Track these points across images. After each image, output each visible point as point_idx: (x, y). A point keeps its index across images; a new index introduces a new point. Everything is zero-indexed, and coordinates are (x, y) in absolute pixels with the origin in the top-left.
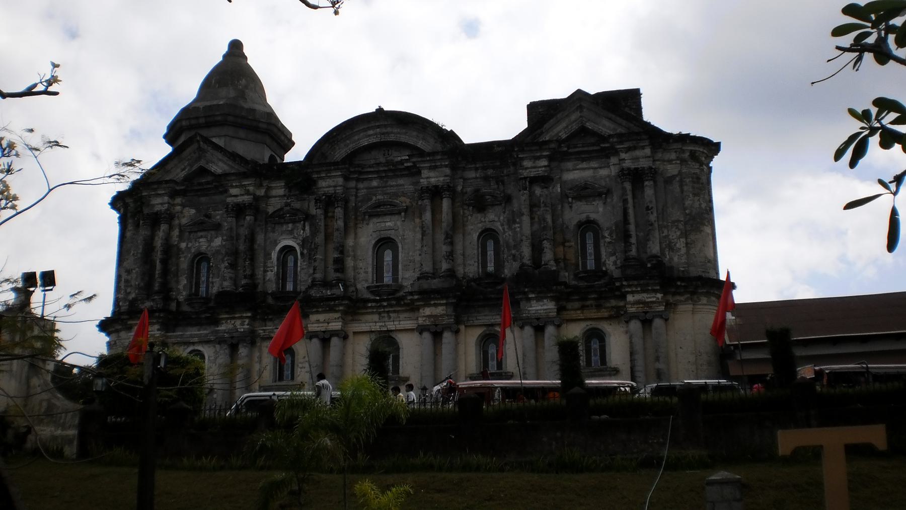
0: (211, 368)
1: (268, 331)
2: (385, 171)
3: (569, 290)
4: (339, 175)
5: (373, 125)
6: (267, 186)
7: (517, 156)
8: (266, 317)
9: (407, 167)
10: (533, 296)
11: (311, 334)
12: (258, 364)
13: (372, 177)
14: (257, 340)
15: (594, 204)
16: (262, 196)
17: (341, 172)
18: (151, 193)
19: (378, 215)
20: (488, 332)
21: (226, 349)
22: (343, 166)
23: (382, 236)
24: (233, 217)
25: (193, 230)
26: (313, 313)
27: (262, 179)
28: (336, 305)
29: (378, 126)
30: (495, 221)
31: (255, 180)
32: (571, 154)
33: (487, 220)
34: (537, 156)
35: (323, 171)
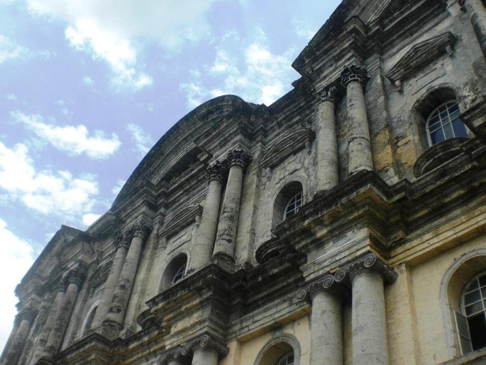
2: (187, 180)
3: (397, 197)
4: (143, 203)
5: (181, 140)
6: (97, 250)
7: (313, 71)
10: (324, 231)
13: (179, 196)
15: (436, 68)
20: (273, 343)
22: (143, 190)
23: (175, 255)
24: (61, 291)
27: (92, 243)
29: (185, 139)
30: (296, 170)
31: (83, 246)
32: (391, 32)
33: (287, 173)
34: (337, 55)
35: (128, 206)
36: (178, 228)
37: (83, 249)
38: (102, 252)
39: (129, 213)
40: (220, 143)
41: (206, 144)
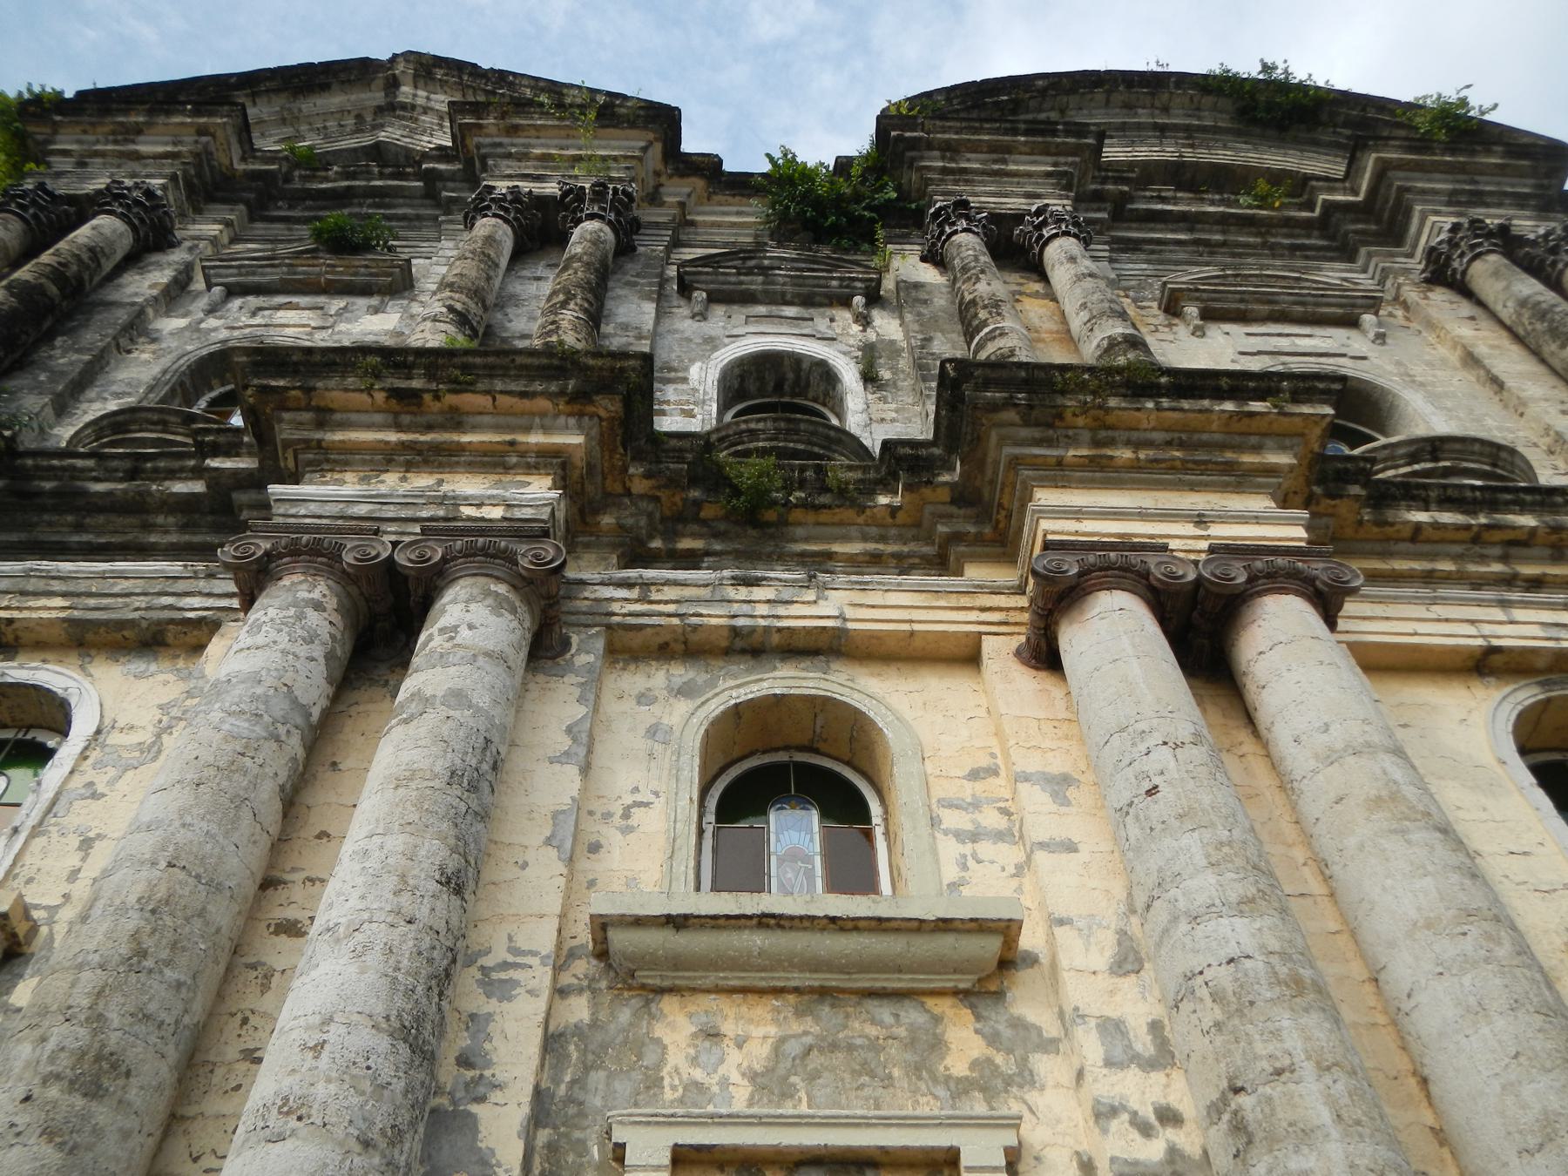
0: (95, 796)
1: (670, 593)
2: (1223, 221)
4: (1048, 175)
6: (682, 205)
8: (656, 544)
9: (1330, 207)
11: (1091, 558)
12: (572, 771)
13: (1159, 242)
14: (575, 639)
16: (657, 225)
17: (1055, 164)
18: (99, 147)
19: (1241, 317)
21: (318, 606)
25: (256, 279)
26: (1060, 475)
28: (1246, 434)
31: (644, 149)
35: (975, 148)
36: (1264, 309)
37: (640, 159)
38: (692, 224)
39: (964, 171)
40: (1454, 193)
41: (1400, 166)
